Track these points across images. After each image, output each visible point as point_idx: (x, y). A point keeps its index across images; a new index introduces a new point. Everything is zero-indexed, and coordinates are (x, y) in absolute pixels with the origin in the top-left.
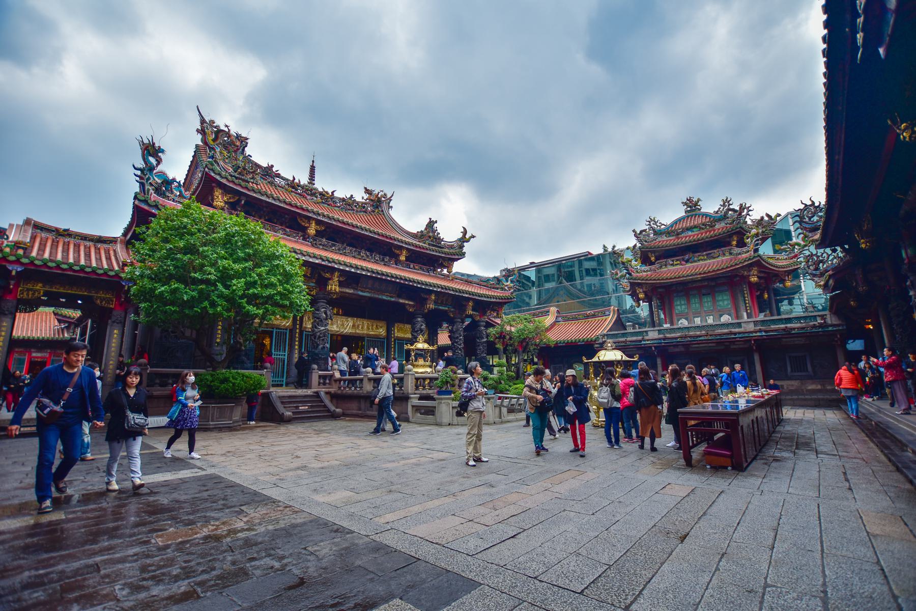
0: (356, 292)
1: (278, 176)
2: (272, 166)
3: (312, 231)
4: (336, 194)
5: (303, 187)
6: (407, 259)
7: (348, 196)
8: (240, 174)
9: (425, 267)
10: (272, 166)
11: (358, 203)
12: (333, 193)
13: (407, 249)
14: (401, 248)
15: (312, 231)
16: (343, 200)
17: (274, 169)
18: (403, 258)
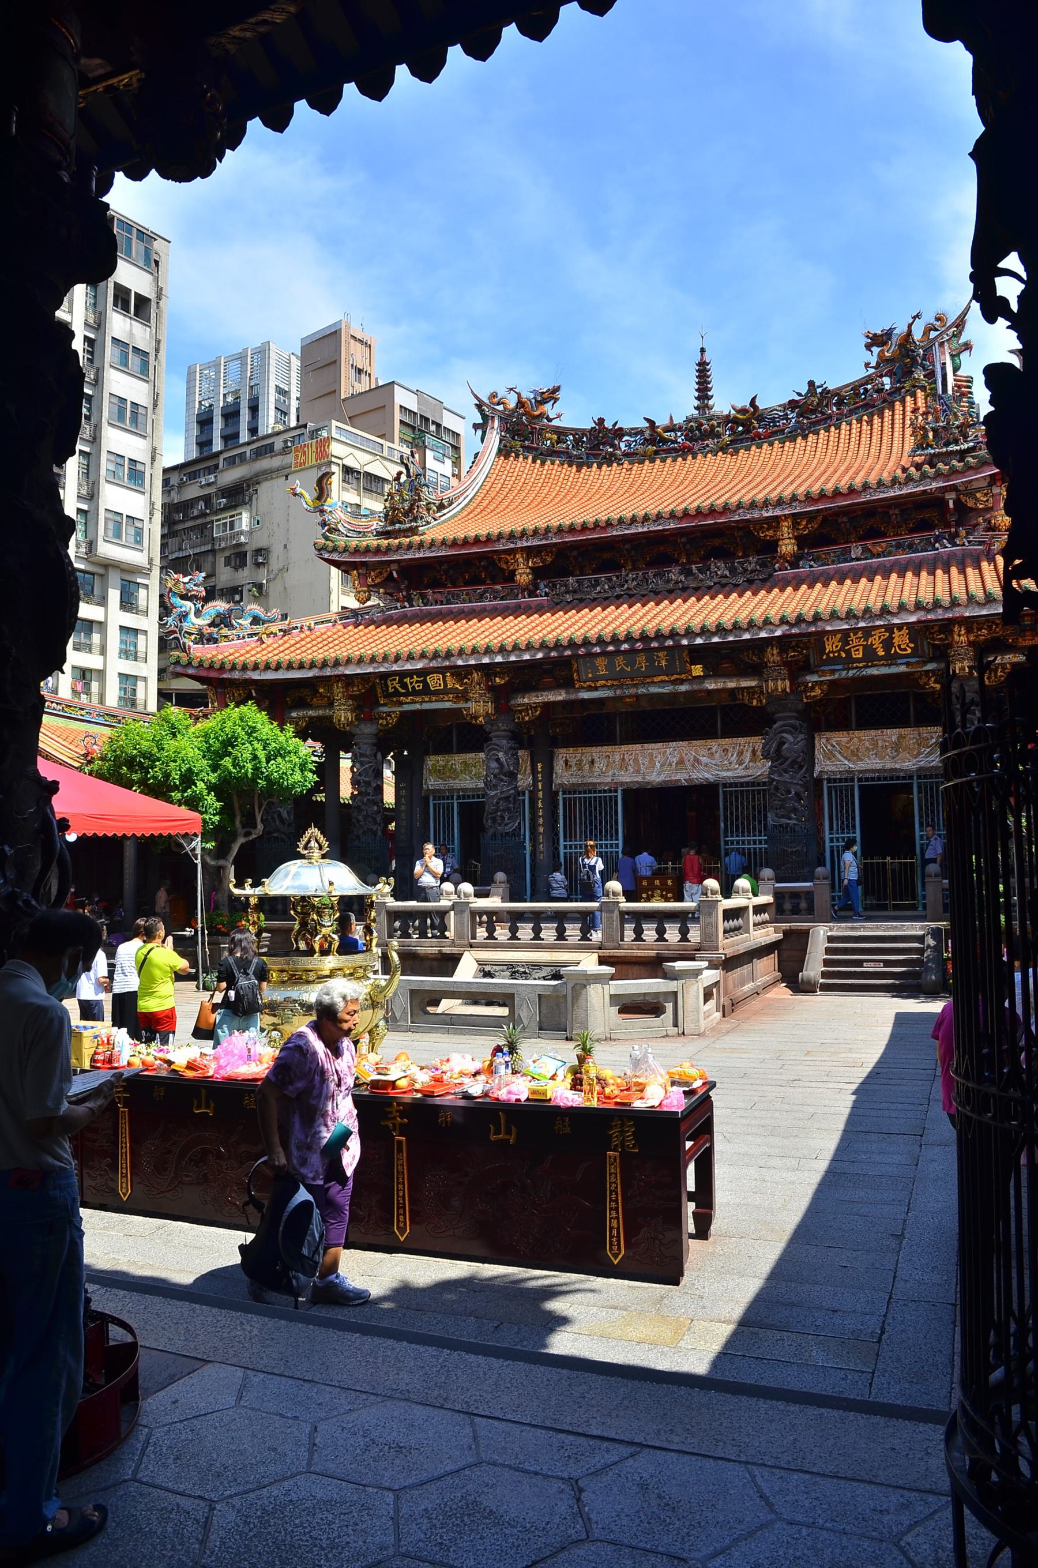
0: (573, 697)
1: (619, 433)
2: (601, 421)
3: (523, 577)
4: (761, 405)
5: (680, 429)
6: (801, 541)
7: (804, 390)
8: (393, 523)
9: (916, 538)
10: (601, 421)
11: (837, 392)
12: (753, 402)
13: (795, 517)
14: (775, 522)
15: (523, 577)
16: (792, 404)
17: (608, 425)
18: (788, 547)
